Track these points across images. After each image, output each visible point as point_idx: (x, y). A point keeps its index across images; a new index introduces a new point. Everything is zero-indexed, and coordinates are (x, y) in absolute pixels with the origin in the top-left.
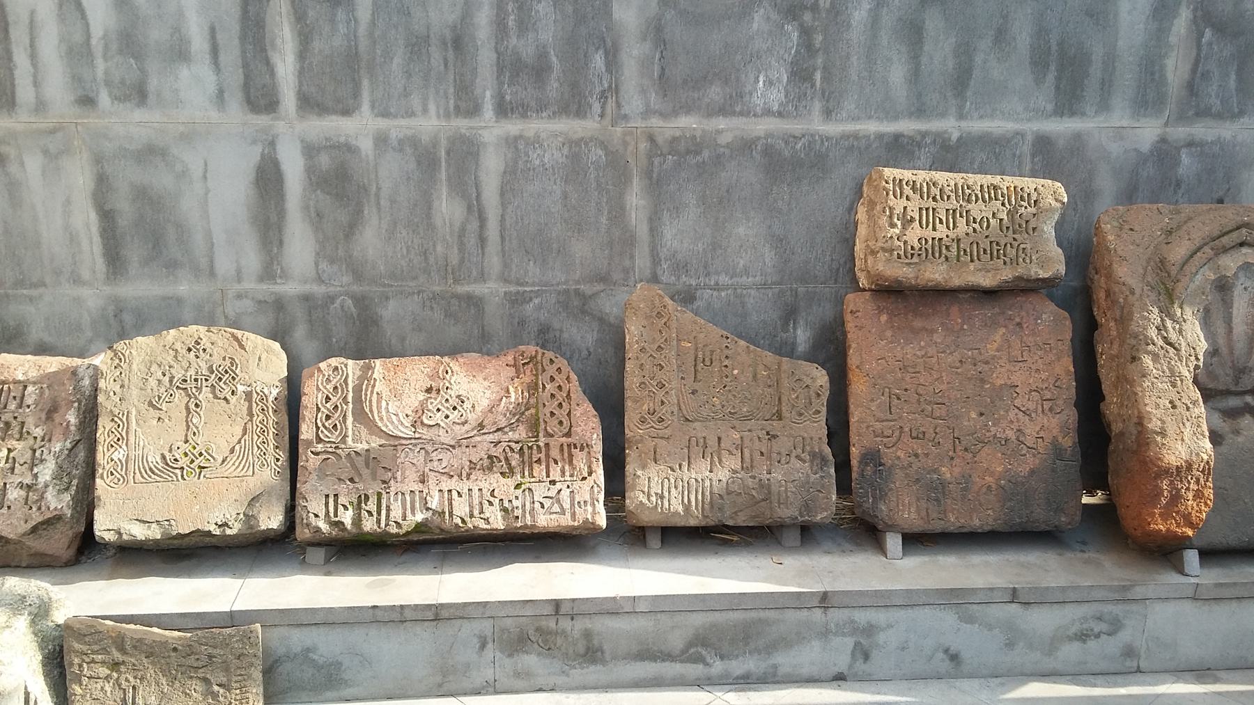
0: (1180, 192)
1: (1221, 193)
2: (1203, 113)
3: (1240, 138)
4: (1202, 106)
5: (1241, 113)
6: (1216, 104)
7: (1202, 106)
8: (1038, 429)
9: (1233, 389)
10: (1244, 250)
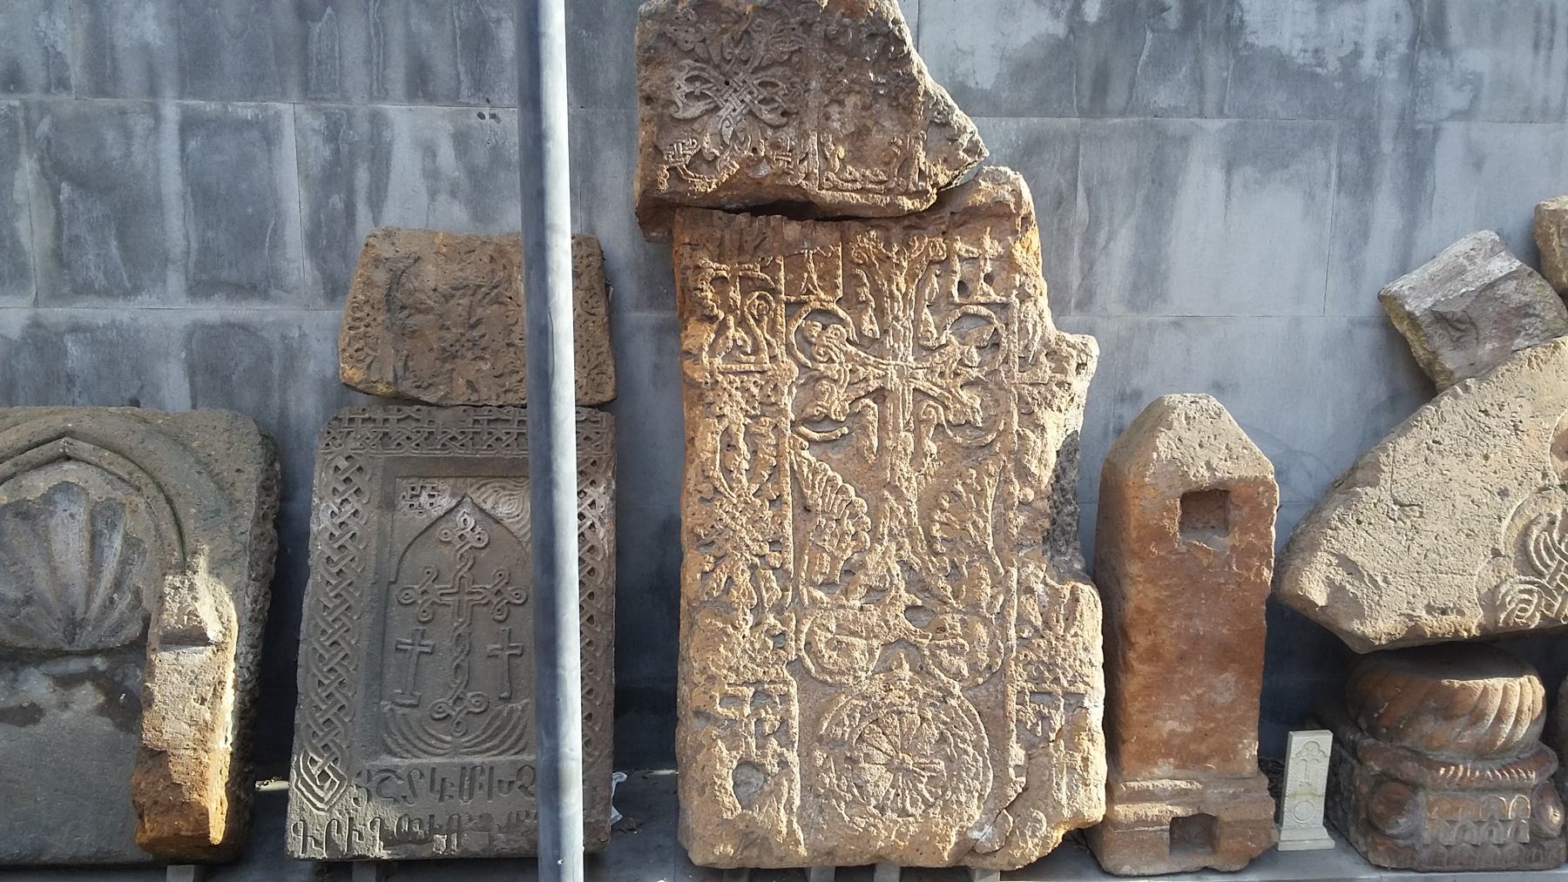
0: (76, 391)
1: (134, 392)
2: (83, 289)
3: (142, 321)
4: (80, 280)
5: (136, 290)
6: (100, 280)
7: (80, 280)
9: (67, 648)
10: (67, 466)
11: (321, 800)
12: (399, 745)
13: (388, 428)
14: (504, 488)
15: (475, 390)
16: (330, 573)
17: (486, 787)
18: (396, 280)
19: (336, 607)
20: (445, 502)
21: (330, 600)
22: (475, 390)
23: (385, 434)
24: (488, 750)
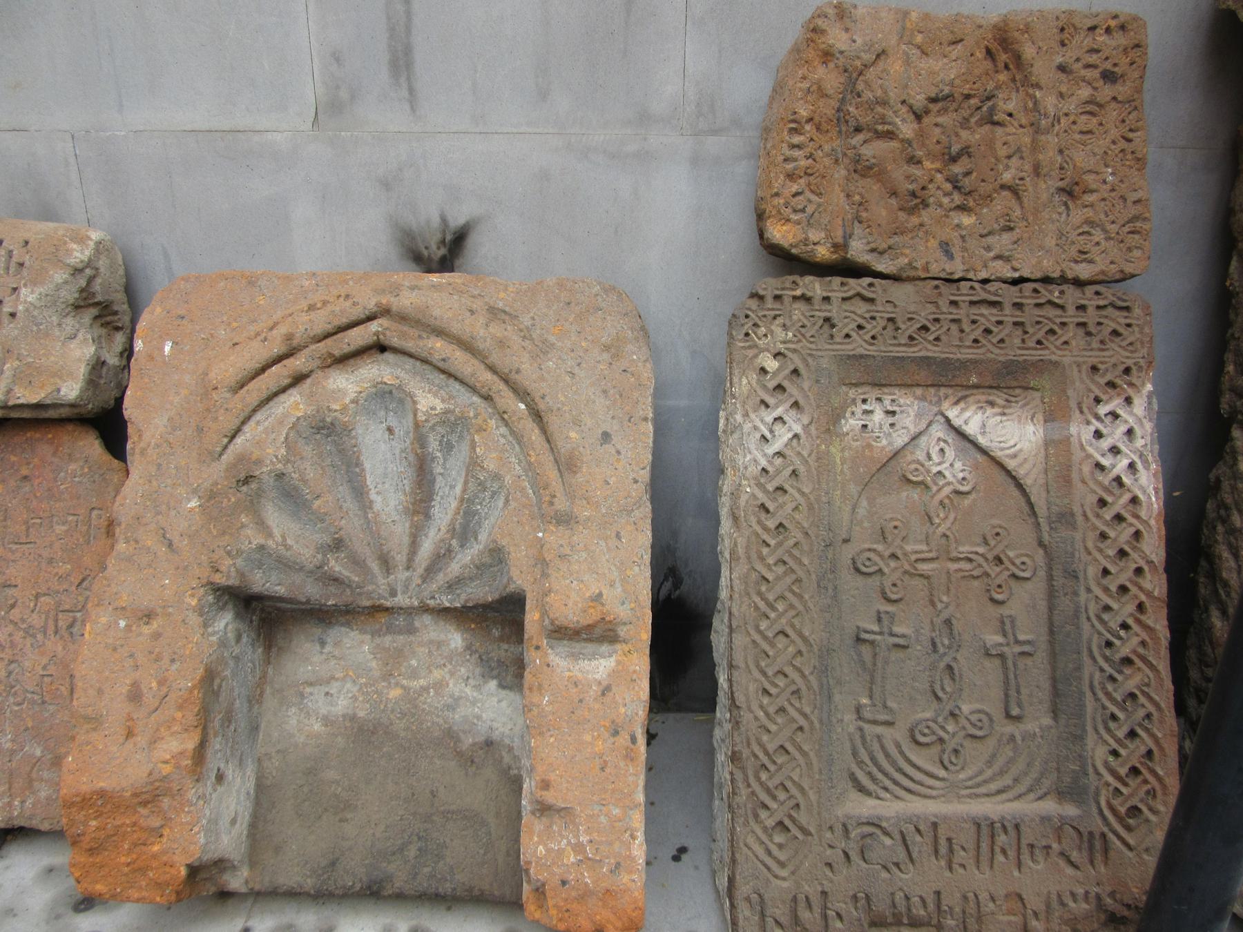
8: (45, 661)
11: (782, 865)
12: (874, 779)
13: (834, 311)
14: (992, 404)
15: (951, 257)
16: (765, 529)
17: (1012, 853)
18: (851, 89)
19: (778, 578)
20: (908, 422)
21: (769, 567)
22: (951, 257)
23: (827, 320)
24: (999, 792)
